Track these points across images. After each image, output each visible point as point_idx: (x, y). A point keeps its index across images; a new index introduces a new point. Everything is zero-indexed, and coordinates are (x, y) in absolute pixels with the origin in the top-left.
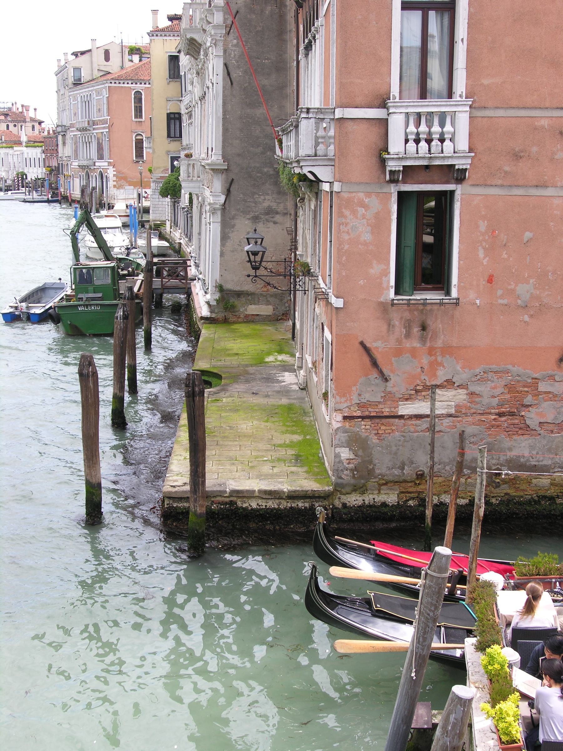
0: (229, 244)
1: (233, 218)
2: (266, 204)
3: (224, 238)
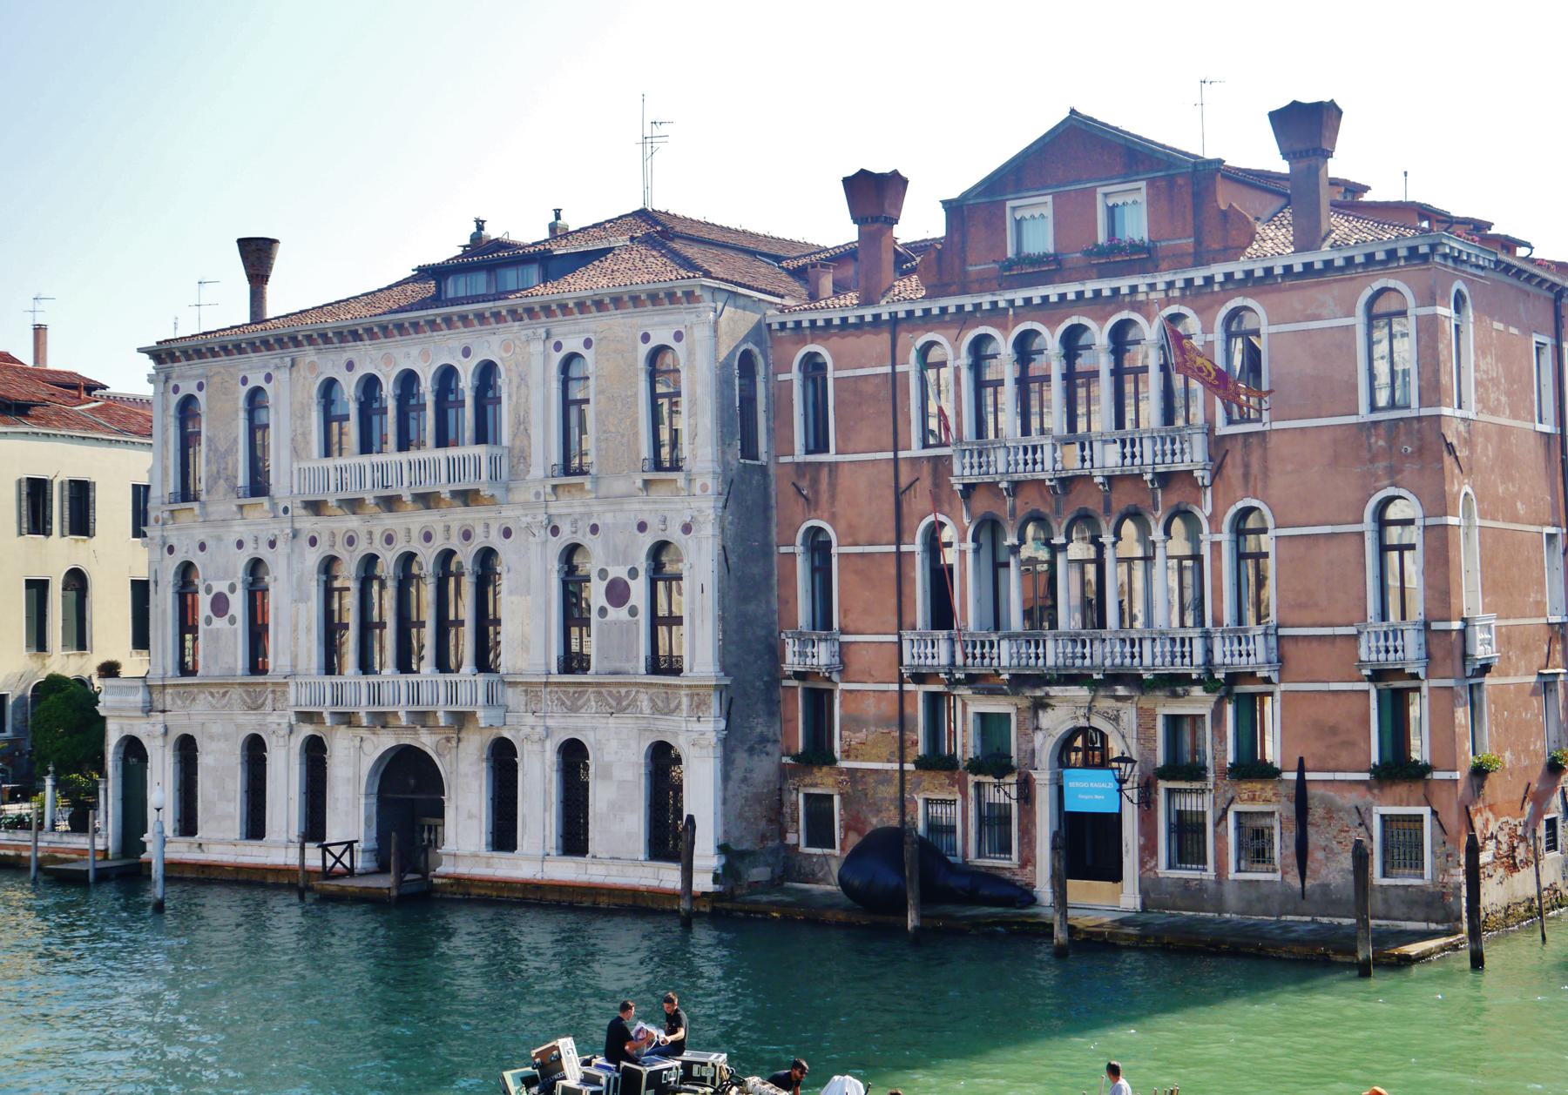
0: (731, 784)
1: (733, 751)
2: (759, 730)
3: (726, 778)
